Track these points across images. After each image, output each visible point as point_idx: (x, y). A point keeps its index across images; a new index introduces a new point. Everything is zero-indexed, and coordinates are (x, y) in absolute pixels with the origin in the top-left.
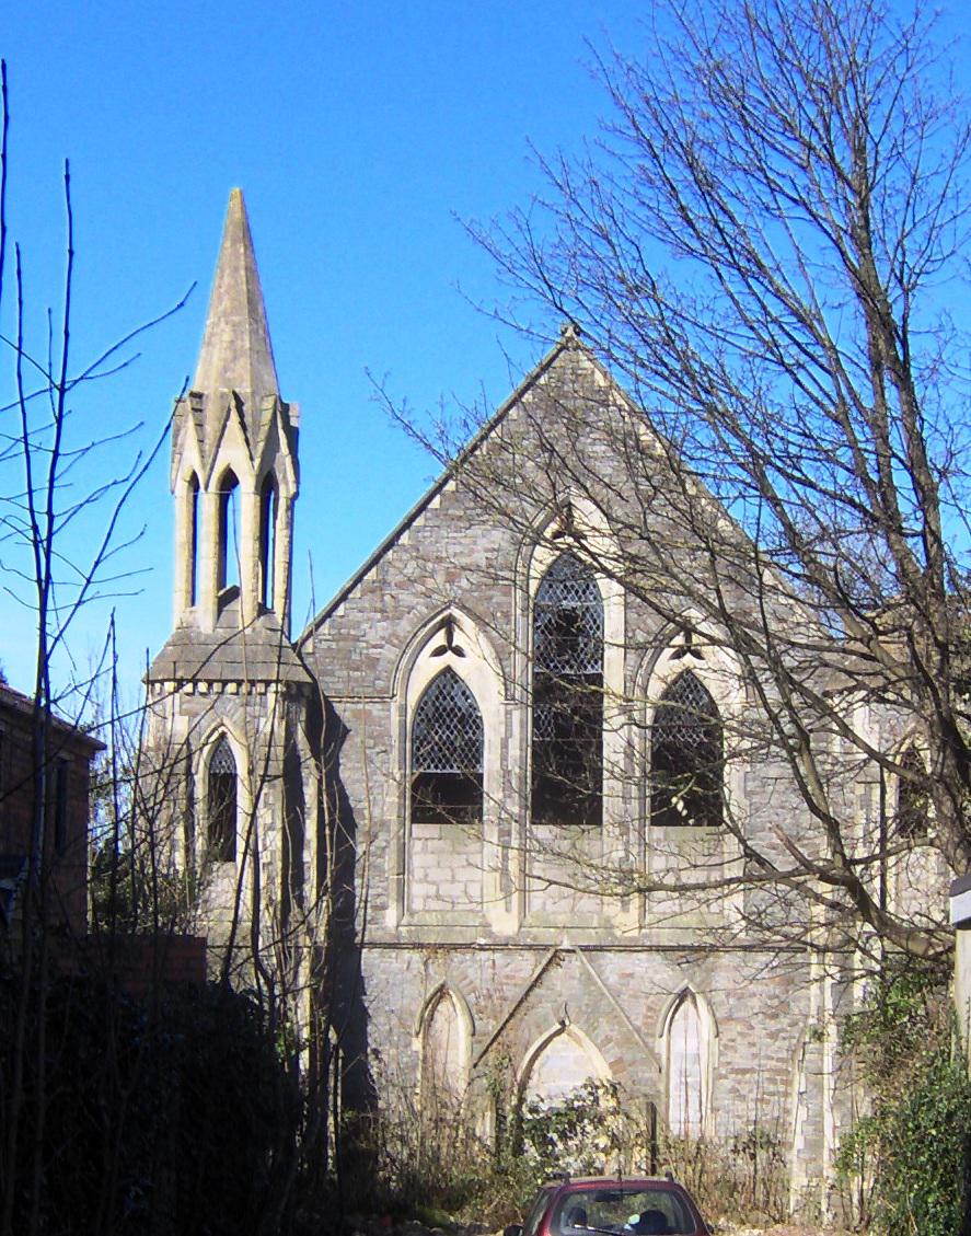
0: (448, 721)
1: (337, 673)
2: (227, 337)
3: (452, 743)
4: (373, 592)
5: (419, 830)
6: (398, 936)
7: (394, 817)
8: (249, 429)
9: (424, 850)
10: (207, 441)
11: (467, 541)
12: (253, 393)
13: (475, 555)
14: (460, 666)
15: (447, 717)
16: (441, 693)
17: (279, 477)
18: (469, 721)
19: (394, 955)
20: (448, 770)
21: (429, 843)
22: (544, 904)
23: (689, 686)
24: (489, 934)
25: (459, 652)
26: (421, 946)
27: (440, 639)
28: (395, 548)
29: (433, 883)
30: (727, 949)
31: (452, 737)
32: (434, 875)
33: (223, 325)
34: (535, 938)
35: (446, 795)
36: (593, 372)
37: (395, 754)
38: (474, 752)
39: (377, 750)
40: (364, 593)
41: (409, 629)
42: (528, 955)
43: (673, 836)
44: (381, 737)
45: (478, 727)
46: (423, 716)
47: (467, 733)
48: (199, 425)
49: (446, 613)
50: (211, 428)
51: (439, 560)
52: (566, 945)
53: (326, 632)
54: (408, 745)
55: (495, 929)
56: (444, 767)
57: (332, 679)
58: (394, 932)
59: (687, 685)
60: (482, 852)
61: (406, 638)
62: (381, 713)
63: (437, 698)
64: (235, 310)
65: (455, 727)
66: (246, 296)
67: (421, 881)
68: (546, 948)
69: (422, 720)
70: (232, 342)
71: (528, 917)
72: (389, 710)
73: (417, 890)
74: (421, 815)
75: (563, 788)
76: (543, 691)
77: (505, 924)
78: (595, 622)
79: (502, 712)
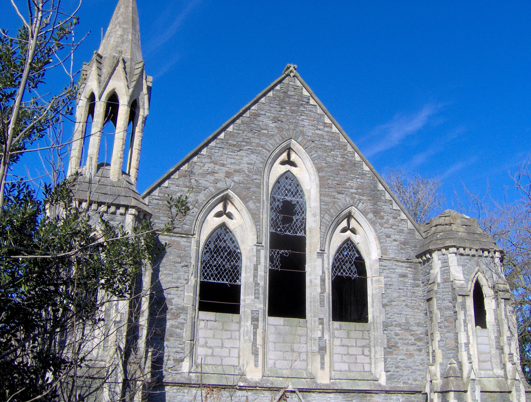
0: (222, 254)
1: (162, 218)
2: (119, 33)
3: (224, 266)
4: (185, 176)
5: (204, 315)
6: (190, 378)
7: (190, 305)
8: (128, 74)
9: (206, 327)
10: (103, 76)
11: (238, 157)
12: (131, 59)
13: (242, 165)
14: (231, 224)
15: (221, 253)
16: (219, 237)
17: (141, 104)
18: (234, 255)
19: (186, 391)
20: (221, 281)
21: (209, 322)
22: (275, 363)
23: (349, 247)
24: (246, 380)
25: (230, 216)
26: (205, 386)
27: (219, 208)
28: (199, 156)
29: (210, 348)
30: (377, 392)
31: (224, 263)
32: (211, 343)
33: (118, 28)
34: (272, 383)
35: (218, 296)
36: (302, 89)
37: (191, 269)
38: (236, 273)
39: (182, 264)
40: (180, 176)
41: (204, 199)
42: (267, 393)
43: (344, 327)
44: (184, 257)
45: (239, 258)
46: (208, 249)
47: (232, 261)
48: (99, 69)
49: (225, 193)
50: (106, 71)
51: (223, 165)
52: (290, 388)
53: (157, 194)
54: (199, 264)
55: (248, 377)
56: (219, 280)
57: (159, 221)
58: (187, 376)
59: (349, 246)
60: (239, 330)
61: (202, 203)
62: (186, 243)
63: (216, 240)
64: (125, 22)
65: (226, 257)
66: (131, 18)
67: (202, 346)
68: (278, 389)
69: (207, 252)
70: (122, 36)
71: (266, 371)
72: (190, 242)
73: (200, 351)
74: (203, 307)
75: (286, 297)
76: (277, 241)
77: (254, 375)
78: (301, 209)
79: (255, 250)
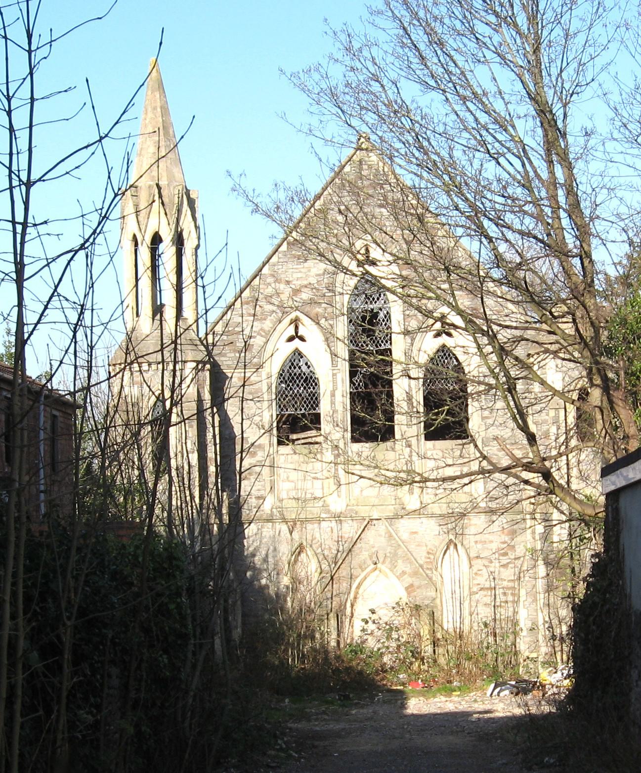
0: (297, 381)
3: (300, 395)
15: (297, 381)
16: (292, 364)
18: (310, 381)
24: (329, 512)
25: (302, 339)
31: (301, 391)
35: (297, 421)
38: (314, 400)
41: (271, 325)
45: (316, 384)
46: (282, 379)
47: (310, 388)
51: (288, 282)
63: (290, 368)
65: (302, 385)
69: (281, 382)
